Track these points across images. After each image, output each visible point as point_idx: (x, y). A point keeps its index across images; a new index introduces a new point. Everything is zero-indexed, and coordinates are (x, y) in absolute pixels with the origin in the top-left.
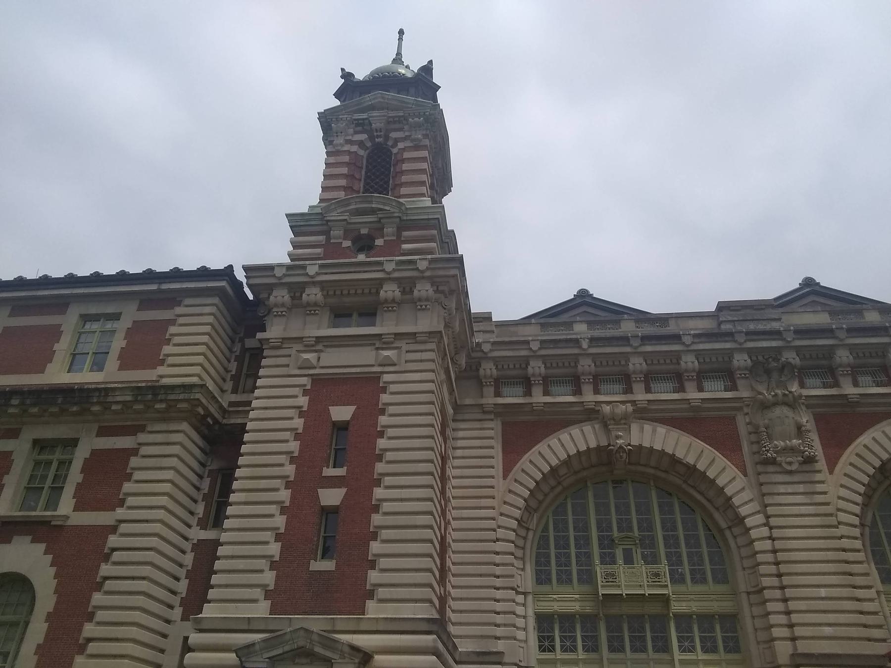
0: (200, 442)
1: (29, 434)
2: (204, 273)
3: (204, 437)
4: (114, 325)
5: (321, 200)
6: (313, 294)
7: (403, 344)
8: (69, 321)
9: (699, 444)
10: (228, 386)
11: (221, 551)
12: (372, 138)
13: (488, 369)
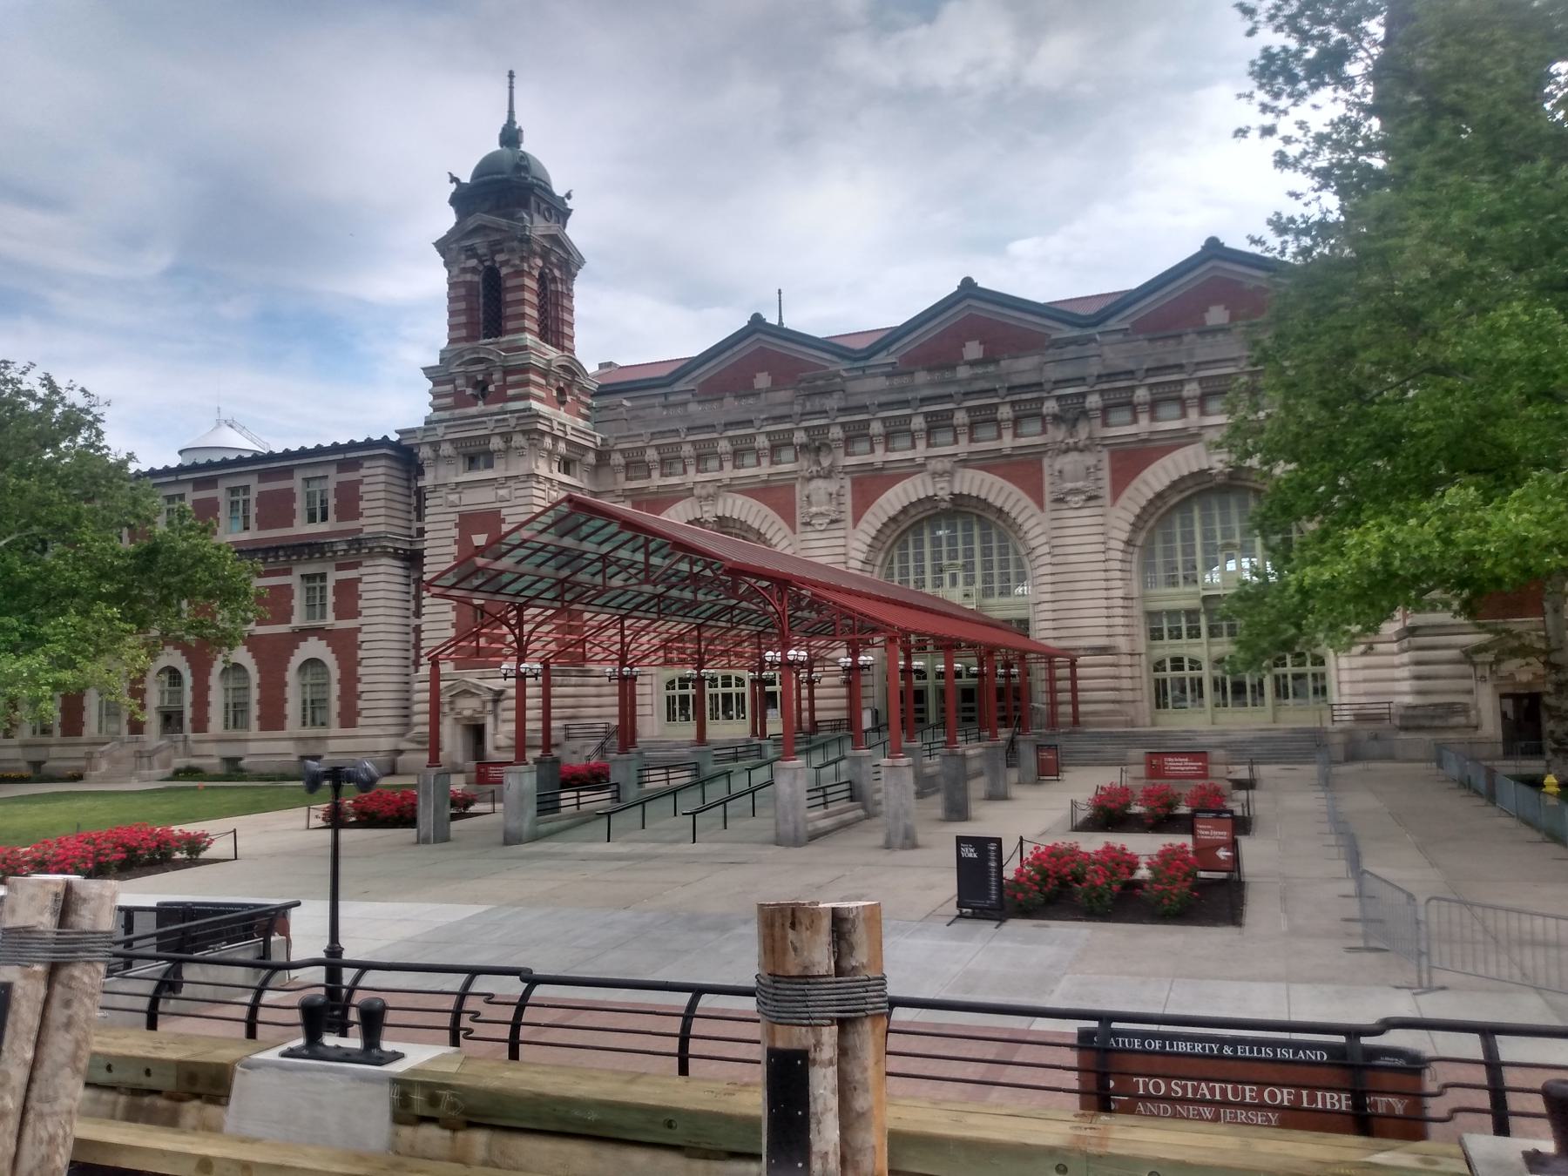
0: (400, 564)
1: (299, 570)
2: (369, 444)
3: (403, 560)
4: (323, 485)
5: (451, 341)
6: (446, 449)
7: (510, 483)
8: (296, 483)
9: (766, 510)
10: (413, 516)
11: (423, 636)
12: (482, 262)
13: (617, 459)
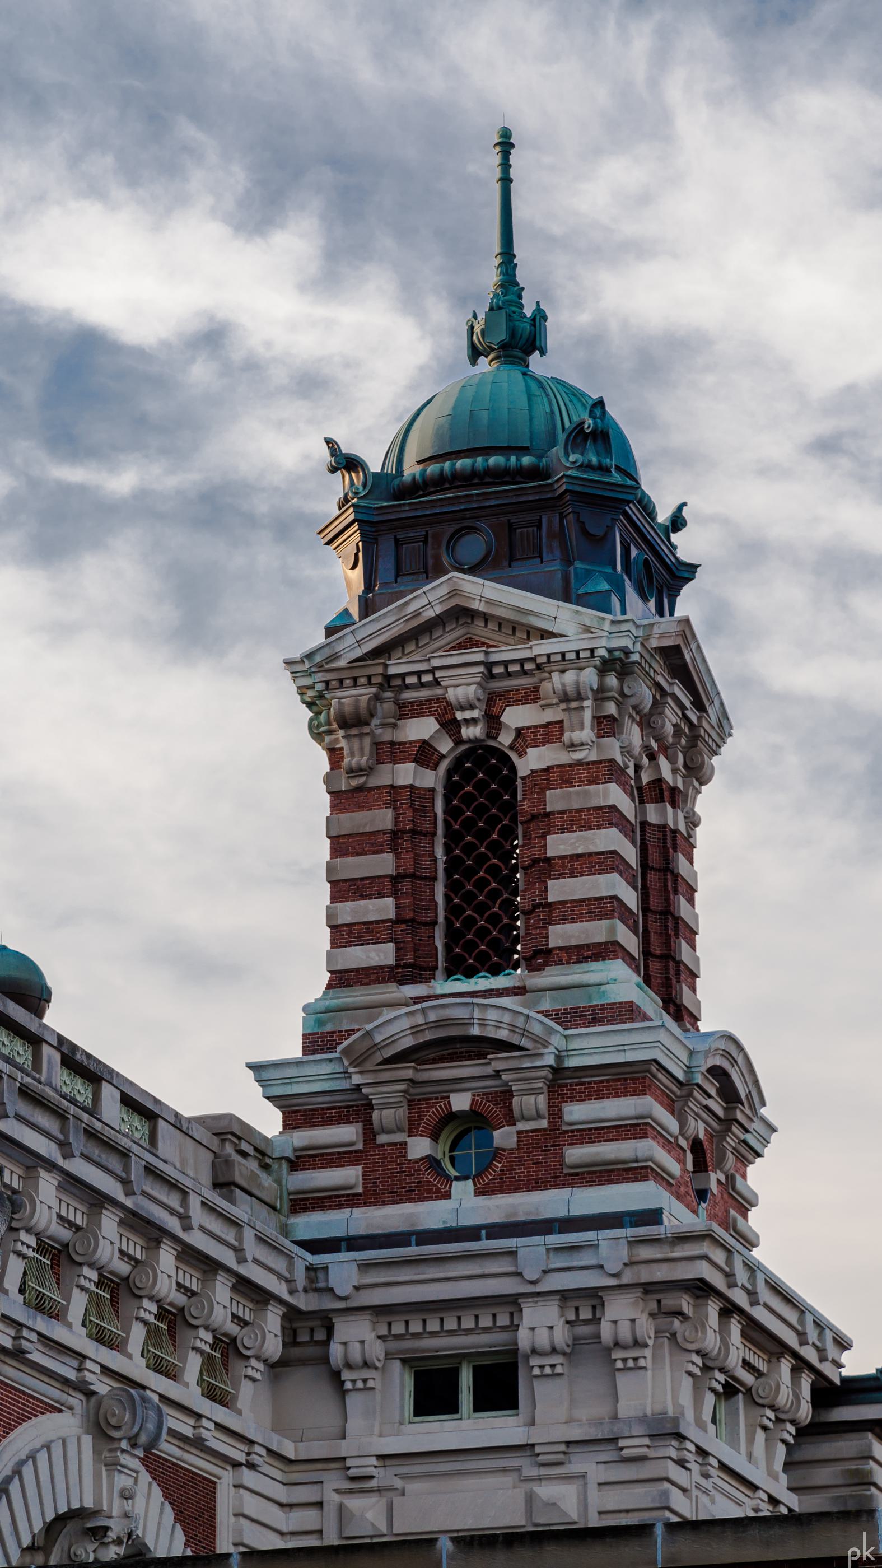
12: (450, 726)
